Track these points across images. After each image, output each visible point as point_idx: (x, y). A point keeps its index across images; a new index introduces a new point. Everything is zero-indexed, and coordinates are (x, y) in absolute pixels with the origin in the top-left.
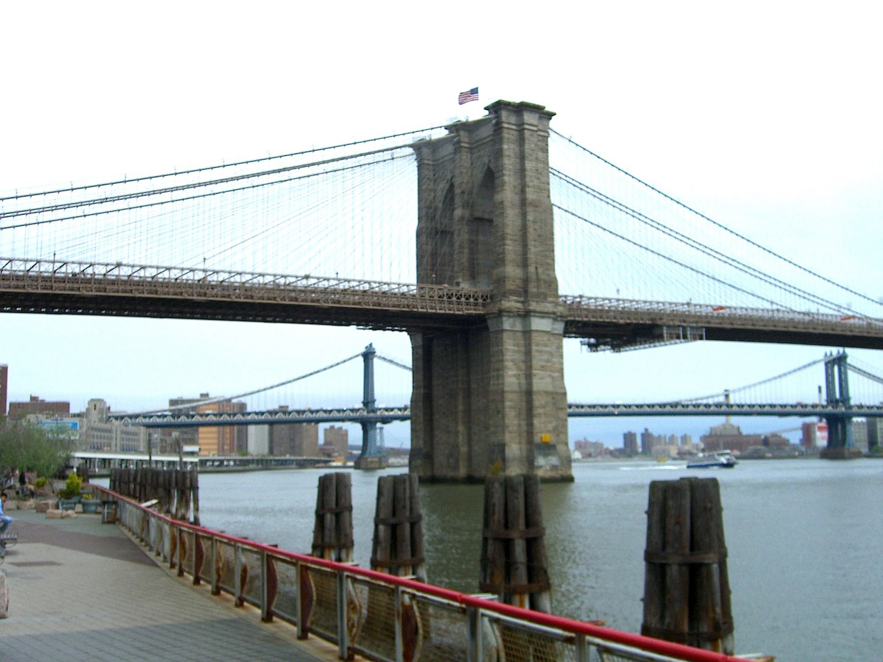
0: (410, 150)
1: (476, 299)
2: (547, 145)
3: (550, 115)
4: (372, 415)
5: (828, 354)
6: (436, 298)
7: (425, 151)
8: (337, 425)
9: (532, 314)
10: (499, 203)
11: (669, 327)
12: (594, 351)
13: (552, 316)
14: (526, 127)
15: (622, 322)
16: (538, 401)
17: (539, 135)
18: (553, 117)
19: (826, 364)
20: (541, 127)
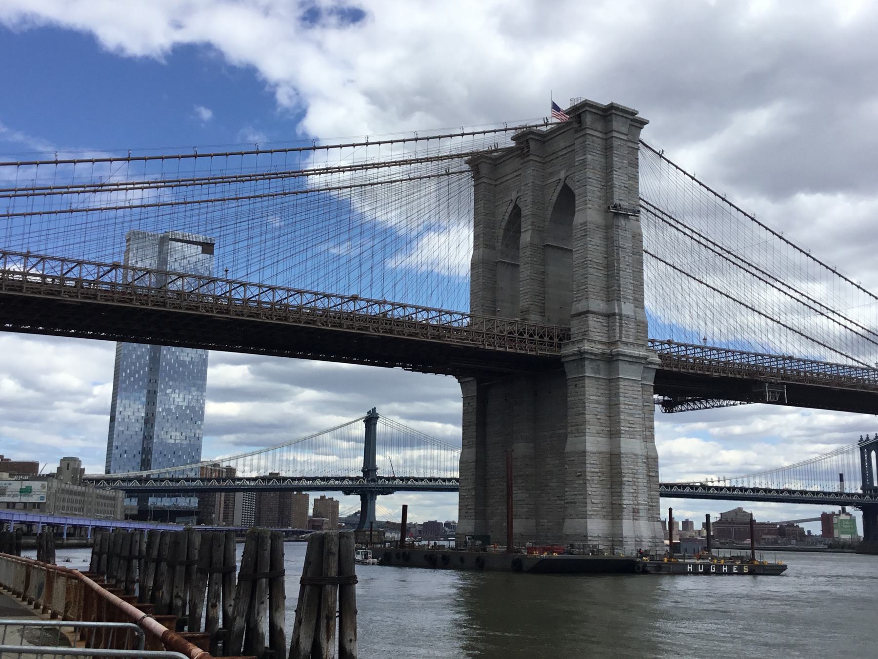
0: (466, 167)
1: (551, 338)
2: (638, 159)
3: (643, 123)
4: (372, 484)
5: (864, 438)
6: (506, 333)
7: (484, 169)
8: (328, 495)
9: (621, 358)
10: (581, 224)
11: (771, 383)
12: (669, 412)
13: (643, 361)
14: (615, 134)
15: (715, 375)
16: (627, 466)
17: (628, 147)
18: (645, 126)
19: (862, 449)
20: (630, 137)
